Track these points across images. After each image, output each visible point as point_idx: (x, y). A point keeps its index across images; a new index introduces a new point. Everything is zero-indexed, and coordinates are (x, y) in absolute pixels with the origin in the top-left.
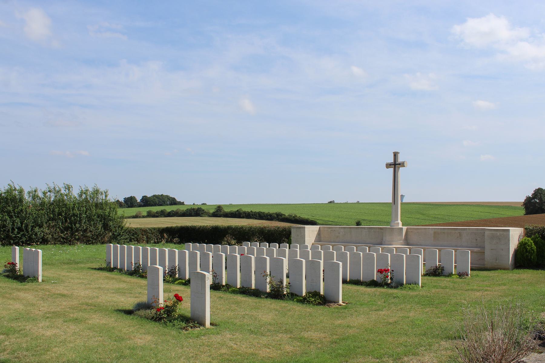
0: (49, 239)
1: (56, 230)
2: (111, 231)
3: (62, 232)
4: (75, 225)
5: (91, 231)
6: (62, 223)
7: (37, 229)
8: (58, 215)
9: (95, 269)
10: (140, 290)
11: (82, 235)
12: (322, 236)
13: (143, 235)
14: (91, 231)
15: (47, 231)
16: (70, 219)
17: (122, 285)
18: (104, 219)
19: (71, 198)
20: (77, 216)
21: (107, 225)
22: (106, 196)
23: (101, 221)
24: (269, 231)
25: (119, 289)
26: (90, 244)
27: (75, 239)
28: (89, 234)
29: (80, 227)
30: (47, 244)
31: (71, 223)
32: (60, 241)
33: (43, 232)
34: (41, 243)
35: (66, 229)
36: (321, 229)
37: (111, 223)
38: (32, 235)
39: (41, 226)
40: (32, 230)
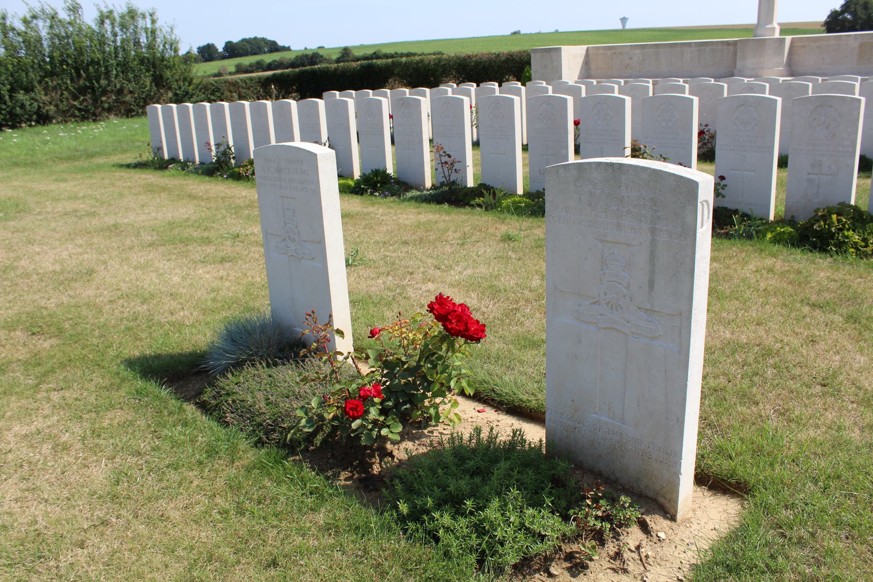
0: (51, 113)
1: (62, 94)
2: (170, 88)
3: (75, 98)
4: (98, 82)
5: (131, 92)
6: (72, 80)
7: (21, 96)
8: (61, 64)
9: (128, 166)
10: (236, 226)
11: (116, 101)
12: (593, 66)
13: (230, 91)
14: (131, 92)
15: (44, 97)
16: (86, 70)
17: (185, 211)
18: (154, 66)
19: (80, 30)
20: (98, 63)
21: (161, 76)
22: (153, 22)
23: (148, 71)
24: (478, 63)
25: (172, 225)
26: (132, 116)
27: (103, 109)
28: (128, 98)
29: (109, 85)
30: (51, 122)
31: (89, 79)
32: (75, 116)
33: (36, 100)
34: (38, 122)
35: (83, 91)
36: (590, 52)
37: (168, 74)
38: (14, 108)
39: (28, 89)
40: (11, 97)
